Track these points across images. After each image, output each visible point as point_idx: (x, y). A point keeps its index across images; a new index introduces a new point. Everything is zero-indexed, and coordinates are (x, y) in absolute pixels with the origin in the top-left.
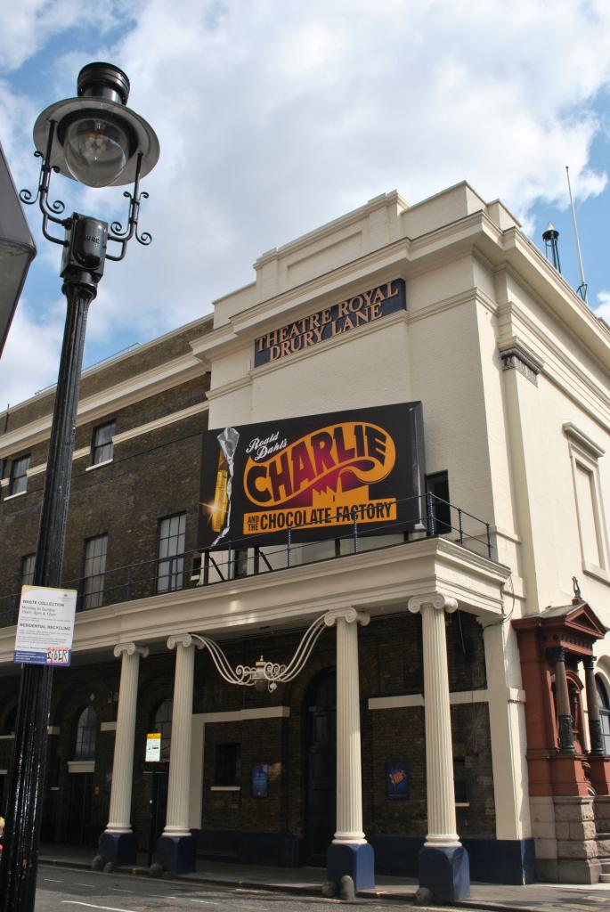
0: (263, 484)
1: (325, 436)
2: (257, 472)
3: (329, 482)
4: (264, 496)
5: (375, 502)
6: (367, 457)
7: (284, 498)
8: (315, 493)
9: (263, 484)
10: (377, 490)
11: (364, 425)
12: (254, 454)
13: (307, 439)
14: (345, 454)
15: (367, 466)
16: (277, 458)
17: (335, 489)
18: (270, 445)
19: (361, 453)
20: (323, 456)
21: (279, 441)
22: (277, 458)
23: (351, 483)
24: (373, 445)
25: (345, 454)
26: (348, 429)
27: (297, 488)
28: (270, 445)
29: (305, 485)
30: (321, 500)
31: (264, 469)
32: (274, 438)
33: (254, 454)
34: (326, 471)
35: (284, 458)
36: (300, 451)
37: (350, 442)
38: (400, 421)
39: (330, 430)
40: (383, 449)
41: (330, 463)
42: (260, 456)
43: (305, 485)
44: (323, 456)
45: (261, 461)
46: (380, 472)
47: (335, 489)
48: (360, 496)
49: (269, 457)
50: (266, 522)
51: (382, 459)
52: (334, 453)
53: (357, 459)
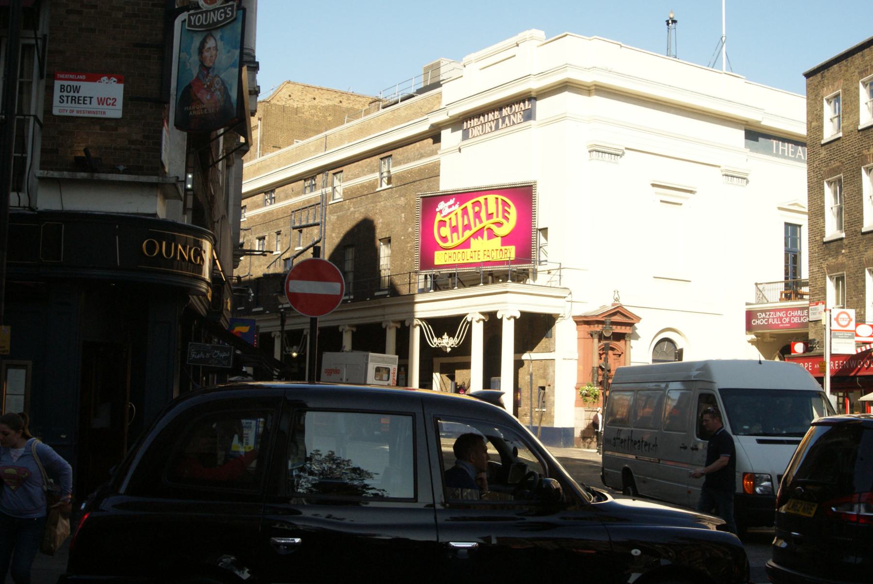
0: (445, 231)
1: (477, 203)
2: (442, 223)
3: (479, 234)
4: (444, 239)
5: (503, 248)
6: (500, 219)
7: (457, 242)
8: (472, 239)
9: (445, 231)
10: (506, 240)
11: (500, 197)
12: (441, 212)
13: (469, 204)
14: (489, 216)
15: (499, 224)
16: (452, 216)
17: (482, 237)
18: (450, 207)
19: (497, 216)
20: (477, 215)
21: (454, 204)
22: (452, 216)
23: (491, 235)
24: (505, 211)
25: (489, 216)
26: (491, 198)
27: (463, 235)
28: (450, 207)
29: (468, 233)
30: (475, 243)
31: (445, 222)
32: (452, 201)
33: (441, 212)
34: (479, 226)
35: (456, 214)
36: (465, 211)
37: (492, 209)
38: (523, 196)
39: (481, 199)
40: (509, 213)
41: (481, 222)
42: (444, 213)
43: (468, 233)
44: (477, 215)
45: (445, 216)
46: (508, 227)
47: (482, 237)
48: (496, 242)
49: (449, 214)
50: (447, 257)
51: (507, 219)
52: (483, 215)
53: (495, 219)
